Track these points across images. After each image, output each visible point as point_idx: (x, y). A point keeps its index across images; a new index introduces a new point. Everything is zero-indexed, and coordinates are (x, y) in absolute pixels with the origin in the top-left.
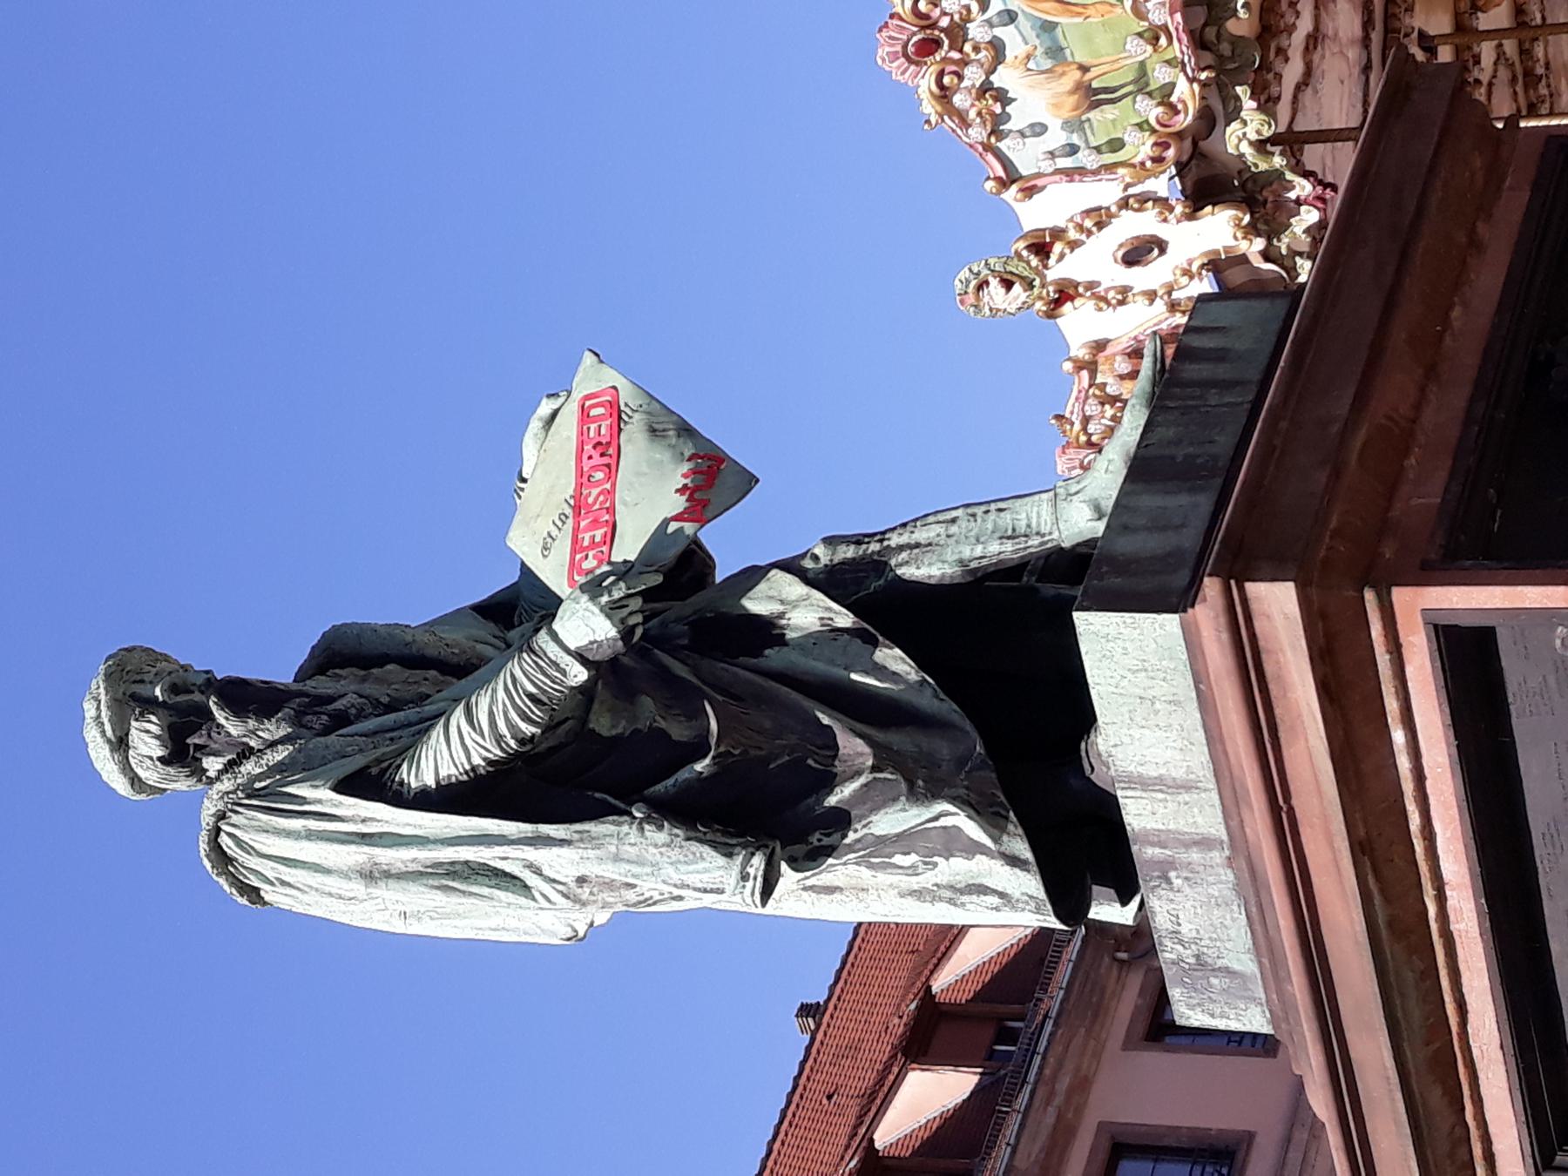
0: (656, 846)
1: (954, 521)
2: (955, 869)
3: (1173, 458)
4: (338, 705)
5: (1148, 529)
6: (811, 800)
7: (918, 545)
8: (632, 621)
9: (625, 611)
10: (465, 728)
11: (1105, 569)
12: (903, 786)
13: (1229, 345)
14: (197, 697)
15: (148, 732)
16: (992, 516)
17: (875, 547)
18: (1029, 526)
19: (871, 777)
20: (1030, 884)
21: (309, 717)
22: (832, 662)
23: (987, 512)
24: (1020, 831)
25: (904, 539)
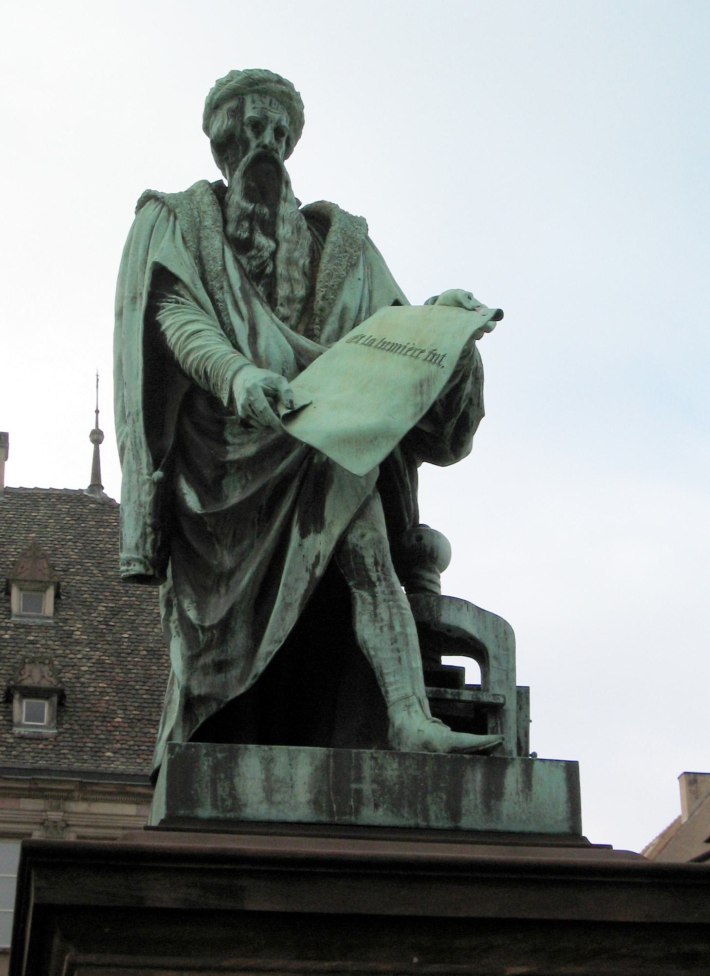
0: (139, 496)
1: (392, 627)
3: (359, 779)
4: (261, 239)
5: (267, 779)
6: (188, 589)
7: (375, 605)
8: (252, 422)
9: (255, 417)
10: (183, 338)
11: (219, 756)
12: (196, 651)
13: (507, 796)
14: (253, 144)
15: (223, 121)
17: (374, 576)
18: (391, 684)
19: (197, 627)
21: (246, 224)
22: (290, 572)
23: (398, 651)
25: (380, 597)
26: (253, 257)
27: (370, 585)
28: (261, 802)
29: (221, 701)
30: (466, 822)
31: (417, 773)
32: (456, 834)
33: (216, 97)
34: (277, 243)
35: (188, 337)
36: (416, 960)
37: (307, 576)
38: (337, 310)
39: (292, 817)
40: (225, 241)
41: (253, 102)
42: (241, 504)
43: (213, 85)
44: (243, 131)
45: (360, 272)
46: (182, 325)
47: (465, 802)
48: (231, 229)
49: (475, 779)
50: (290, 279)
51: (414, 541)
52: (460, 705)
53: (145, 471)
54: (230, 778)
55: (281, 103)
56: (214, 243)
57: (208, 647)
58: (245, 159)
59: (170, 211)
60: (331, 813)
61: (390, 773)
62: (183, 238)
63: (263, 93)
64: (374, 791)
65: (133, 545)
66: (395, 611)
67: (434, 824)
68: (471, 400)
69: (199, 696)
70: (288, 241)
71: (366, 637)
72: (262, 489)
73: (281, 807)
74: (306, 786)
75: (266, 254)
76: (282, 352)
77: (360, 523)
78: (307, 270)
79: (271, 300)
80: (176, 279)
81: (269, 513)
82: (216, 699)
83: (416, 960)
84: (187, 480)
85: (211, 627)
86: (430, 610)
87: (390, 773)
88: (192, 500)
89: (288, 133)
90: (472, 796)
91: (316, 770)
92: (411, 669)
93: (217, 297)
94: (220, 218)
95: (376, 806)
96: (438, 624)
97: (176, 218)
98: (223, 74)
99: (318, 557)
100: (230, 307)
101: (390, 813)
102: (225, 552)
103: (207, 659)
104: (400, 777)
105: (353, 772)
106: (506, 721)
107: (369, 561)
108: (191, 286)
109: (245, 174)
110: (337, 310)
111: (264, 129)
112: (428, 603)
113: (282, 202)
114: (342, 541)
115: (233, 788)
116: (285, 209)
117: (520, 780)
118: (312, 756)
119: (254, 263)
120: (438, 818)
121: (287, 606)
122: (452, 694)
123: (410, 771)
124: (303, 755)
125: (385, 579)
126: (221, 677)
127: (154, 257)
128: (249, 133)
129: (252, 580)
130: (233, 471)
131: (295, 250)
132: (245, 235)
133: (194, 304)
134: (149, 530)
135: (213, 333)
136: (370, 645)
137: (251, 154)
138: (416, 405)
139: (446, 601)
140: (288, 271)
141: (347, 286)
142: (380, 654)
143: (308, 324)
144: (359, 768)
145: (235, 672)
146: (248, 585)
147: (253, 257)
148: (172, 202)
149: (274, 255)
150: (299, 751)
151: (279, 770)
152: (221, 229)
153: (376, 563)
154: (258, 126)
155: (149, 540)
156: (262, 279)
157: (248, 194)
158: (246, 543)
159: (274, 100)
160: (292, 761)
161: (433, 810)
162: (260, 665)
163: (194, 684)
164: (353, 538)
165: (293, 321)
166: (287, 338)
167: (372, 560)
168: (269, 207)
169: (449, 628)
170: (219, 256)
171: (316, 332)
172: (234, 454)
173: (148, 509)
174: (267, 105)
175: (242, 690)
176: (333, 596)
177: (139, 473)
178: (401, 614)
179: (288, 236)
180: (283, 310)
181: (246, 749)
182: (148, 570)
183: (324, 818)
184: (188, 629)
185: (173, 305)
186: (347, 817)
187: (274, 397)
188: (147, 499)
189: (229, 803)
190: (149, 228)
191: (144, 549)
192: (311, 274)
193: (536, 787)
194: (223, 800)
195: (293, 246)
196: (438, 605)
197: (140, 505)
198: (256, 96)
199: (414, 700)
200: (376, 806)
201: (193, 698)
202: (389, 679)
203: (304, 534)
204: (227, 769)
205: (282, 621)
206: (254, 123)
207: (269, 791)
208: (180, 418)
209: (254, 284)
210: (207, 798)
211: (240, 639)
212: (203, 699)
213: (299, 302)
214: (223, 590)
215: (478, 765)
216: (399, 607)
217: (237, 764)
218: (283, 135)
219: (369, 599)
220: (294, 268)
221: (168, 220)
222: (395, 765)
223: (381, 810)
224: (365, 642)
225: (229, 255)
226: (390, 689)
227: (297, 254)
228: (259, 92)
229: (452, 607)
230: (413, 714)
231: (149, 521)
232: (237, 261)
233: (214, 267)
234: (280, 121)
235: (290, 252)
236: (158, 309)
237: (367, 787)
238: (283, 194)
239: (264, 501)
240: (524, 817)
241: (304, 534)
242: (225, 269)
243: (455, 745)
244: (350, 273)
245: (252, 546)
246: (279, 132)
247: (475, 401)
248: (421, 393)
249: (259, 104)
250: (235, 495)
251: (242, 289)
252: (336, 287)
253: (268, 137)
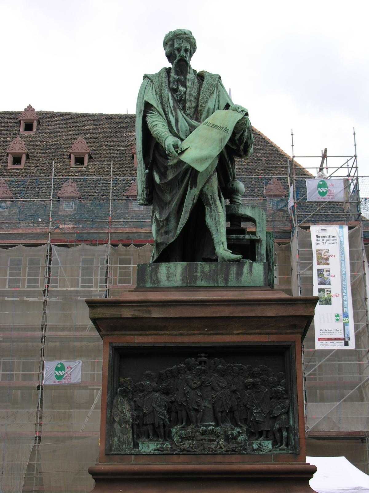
1: (215, 219)
3: (196, 272)
4: (181, 88)
5: (168, 273)
6: (157, 208)
7: (211, 212)
8: (170, 155)
11: (153, 267)
12: (159, 228)
14: (178, 56)
16: (216, 228)
17: (211, 202)
21: (176, 83)
24: (158, 256)
25: (212, 208)
26: (178, 95)
27: (210, 205)
28: (166, 281)
29: (167, 244)
30: (230, 284)
31: (215, 269)
32: (227, 288)
33: (166, 40)
34: (186, 89)
35: (153, 127)
36: (206, 329)
37: (192, 202)
38: (206, 109)
39: (175, 285)
40: (169, 90)
41: (177, 42)
42: (172, 180)
43: (165, 36)
44: (174, 52)
45: (214, 95)
47: (230, 277)
48: (171, 85)
49: (234, 270)
50: (190, 101)
51: (231, 186)
52: (245, 240)
53: (143, 170)
54: (156, 273)
55: (186, 41)
56: (166, 91)
57: (163, 227)
58: (175, 61)
59: (151, 81)
60: (187, 283)
61: (206, 269)
62: (155, 90)
63: (179, 38)
64: (201, 275)
65: (140, 194)
66: (216, 213)
67: (220, 285)
68: (248, 138)
69: (160, 243)
70: (190, 88)
71: (208, 222)
72: (179, 174)
73: (172, 282)
74: (180, 275)
75: (182, 93)
76: (185, 127)
77: (207, 184)
78: (196, 97)
79: (184, 108)
80: (152, 106)
81: (182, 182)
82: (165, 244)
83: (206, 329)
84: (156, 172)
85: (163, 220)
86: (235, 209)
87: (206, 269)
88: (157, 179)
89: (192, 48)
90: (232, 275)
91: (183, 270)
92: (221, 232)
93: (166, 110)
94: (167, 82)
95: (202, 280)
96: (237, 214)
97: (153, 83)
98: (167, 32)
99: (195, 196)
100: (170, 113)
101: (206, 282)
102: (168, 195)
103: (162, 231)
104: (209, 270)
105: (195, 269)
106: (262, 244)
107: (209, 197)
108: (157, 108)
109: (175, 66)
110: (206, 109)
111: (181, 51)
112: (234, 207)
113: (188, 74)
114: (201, 191)
115: (157, 277)
116: (190, 76)
117: (248, 269)
118: (182, 265)
119: (178, 97)
120: (221, 283)
121: (186, 212)
122: (242, 237)
123: (213, 268)
124: (179, 265)
125: (214, 203)
126: (167, 236)
127: (145, 99)
128: (176, 52)
129: (176, 204)
130: (170, 168)
131: (192, 90)
132: (175, 87)
133: (158, 114)
134: (145, 189)
135: (161, 125)
136: (209, 225)
137: (177, 59)
138: (220, 147)
139: (240, 206)
140: (190, 98)
141: (209, 101)
142: (212, 228)
143: (197, 115)
144: (197, 268)
145: (171, 234)
146: (174, 206)
147: (178, 95)
148: (152, 78)
149: (185, 93)
150: (178, 264)
151: (172, 270)
152: (167, 86)
153: (212, 198)
154: (179, 50)
155: (145, 193)
156: (181, 102)
157: (177, 73)
158: (174, 192)
159: (184, 40)
160: (176, 267)
161: (220, 280)
162: (178, 232)
163: (158, 239)
164: (205, 190)
165: (191, 115)
166: (187, 122)
167: (210, 197)
168: (183, 76)
169: (242, 215)
170: (166, 96)
171: (199, 118)
172: (170, 164)
173: (144, 183)
174: (181, 42)
175: (173, 240)
177: (142, 171)
178: (219, 214)
179: (189, 86)
180: (188, 112)
181: (162, 264)
182: (145, 202)
183: (185, 285)
184: (157, 221)
185: (151, 115)
186: (192, 284)
187: (176, 147)
188: (144, 179)
189: (156, 281)
190: (144, 88)
191: (143, 195)
192: (197, 98)
193: (253, 271)
194: (154, 281)
195: (191, 89)
196: (238, 208)
197: (142, 181)
198: (178, 39)
199: (221, 243)
200: (202, 280)
201: (158, 243)
202: (214, 236)
203: (191, 189)
206: (180, 47)
207: (168, 277)
208: (154, 151)
209: (179, 104)
210: (149, 280)
212: (161, 244)
213: (194, 108)
214: (167, 208)
215: (235, 265)
216: (218, 212)
217: (158, 269)
218: (188, 51)
219: (210, 209)
220: (192, 97)
221: (151, 85)
222: (208, 267)
223: (203, 281)
224: (208, 224)
225: (170, 95)
226: (215, 239)
227: (192, 92)
228: (178, 38)
229: (243, 208)
230: (220, 248)
231: (145, 186)
232: (172, 96)
233: (165, 100)
234: (186, 47)
235: (190, 91)
236: (146, 116)
237: (199, 274)
238: (188, 71)
239: (180, 177)
240: (249, 281)
241: (191, 189)
242: (168, 100)
243: (229, 258)
244: (211, 96)
245: (176, 193)
246: (186, 50)
247: (249, 138)
248: (222, 142)
249: (179, 42)
250: (170, 176)
251: (174, 107)
252: (205, 102)
253: (183, 53)
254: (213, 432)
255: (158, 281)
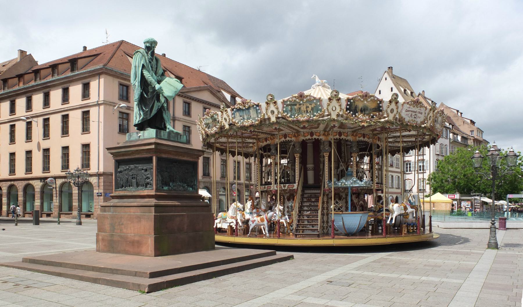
2: (138, 117)
20: (137, 123)
46: (146, 73)
49: (179, 136)
120: (176, 140)
145: (148, 116)
162: (151, 116)
176: (161, 111)
192: (157, 68)
204: (160, 133)
205: (154, 112)
211: (149, 112)
254: (180, 185)
255: (161, 136)
